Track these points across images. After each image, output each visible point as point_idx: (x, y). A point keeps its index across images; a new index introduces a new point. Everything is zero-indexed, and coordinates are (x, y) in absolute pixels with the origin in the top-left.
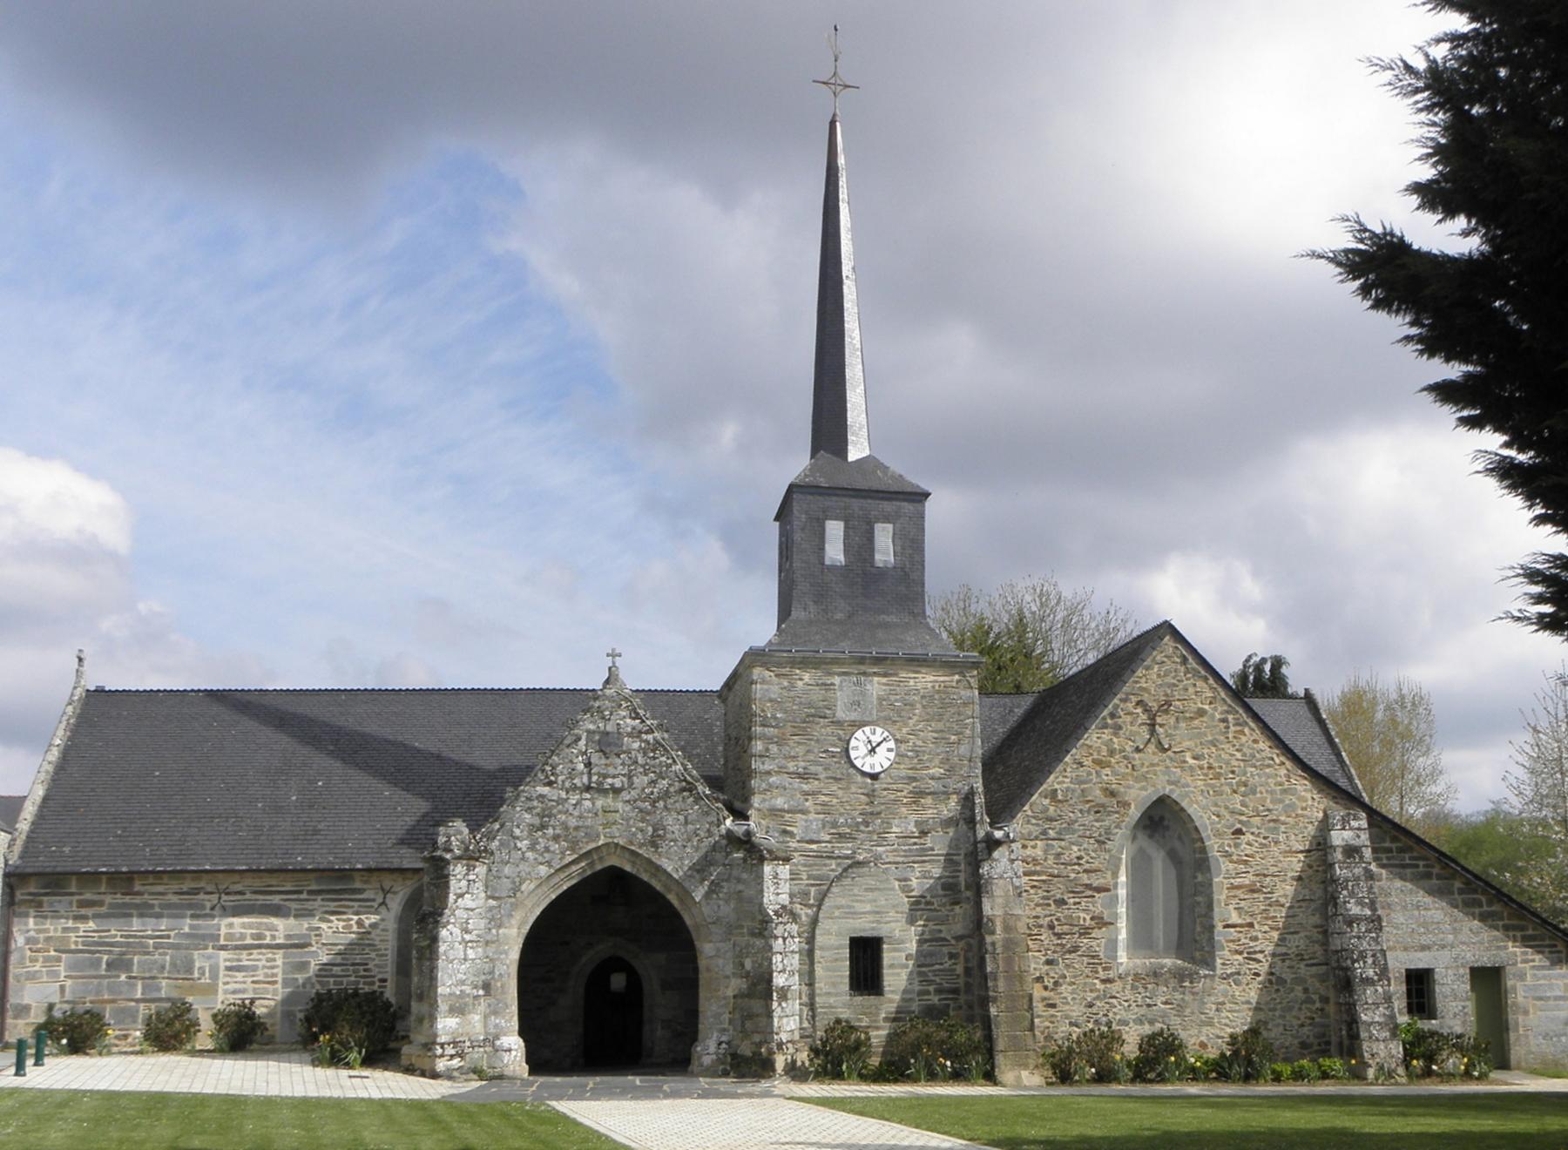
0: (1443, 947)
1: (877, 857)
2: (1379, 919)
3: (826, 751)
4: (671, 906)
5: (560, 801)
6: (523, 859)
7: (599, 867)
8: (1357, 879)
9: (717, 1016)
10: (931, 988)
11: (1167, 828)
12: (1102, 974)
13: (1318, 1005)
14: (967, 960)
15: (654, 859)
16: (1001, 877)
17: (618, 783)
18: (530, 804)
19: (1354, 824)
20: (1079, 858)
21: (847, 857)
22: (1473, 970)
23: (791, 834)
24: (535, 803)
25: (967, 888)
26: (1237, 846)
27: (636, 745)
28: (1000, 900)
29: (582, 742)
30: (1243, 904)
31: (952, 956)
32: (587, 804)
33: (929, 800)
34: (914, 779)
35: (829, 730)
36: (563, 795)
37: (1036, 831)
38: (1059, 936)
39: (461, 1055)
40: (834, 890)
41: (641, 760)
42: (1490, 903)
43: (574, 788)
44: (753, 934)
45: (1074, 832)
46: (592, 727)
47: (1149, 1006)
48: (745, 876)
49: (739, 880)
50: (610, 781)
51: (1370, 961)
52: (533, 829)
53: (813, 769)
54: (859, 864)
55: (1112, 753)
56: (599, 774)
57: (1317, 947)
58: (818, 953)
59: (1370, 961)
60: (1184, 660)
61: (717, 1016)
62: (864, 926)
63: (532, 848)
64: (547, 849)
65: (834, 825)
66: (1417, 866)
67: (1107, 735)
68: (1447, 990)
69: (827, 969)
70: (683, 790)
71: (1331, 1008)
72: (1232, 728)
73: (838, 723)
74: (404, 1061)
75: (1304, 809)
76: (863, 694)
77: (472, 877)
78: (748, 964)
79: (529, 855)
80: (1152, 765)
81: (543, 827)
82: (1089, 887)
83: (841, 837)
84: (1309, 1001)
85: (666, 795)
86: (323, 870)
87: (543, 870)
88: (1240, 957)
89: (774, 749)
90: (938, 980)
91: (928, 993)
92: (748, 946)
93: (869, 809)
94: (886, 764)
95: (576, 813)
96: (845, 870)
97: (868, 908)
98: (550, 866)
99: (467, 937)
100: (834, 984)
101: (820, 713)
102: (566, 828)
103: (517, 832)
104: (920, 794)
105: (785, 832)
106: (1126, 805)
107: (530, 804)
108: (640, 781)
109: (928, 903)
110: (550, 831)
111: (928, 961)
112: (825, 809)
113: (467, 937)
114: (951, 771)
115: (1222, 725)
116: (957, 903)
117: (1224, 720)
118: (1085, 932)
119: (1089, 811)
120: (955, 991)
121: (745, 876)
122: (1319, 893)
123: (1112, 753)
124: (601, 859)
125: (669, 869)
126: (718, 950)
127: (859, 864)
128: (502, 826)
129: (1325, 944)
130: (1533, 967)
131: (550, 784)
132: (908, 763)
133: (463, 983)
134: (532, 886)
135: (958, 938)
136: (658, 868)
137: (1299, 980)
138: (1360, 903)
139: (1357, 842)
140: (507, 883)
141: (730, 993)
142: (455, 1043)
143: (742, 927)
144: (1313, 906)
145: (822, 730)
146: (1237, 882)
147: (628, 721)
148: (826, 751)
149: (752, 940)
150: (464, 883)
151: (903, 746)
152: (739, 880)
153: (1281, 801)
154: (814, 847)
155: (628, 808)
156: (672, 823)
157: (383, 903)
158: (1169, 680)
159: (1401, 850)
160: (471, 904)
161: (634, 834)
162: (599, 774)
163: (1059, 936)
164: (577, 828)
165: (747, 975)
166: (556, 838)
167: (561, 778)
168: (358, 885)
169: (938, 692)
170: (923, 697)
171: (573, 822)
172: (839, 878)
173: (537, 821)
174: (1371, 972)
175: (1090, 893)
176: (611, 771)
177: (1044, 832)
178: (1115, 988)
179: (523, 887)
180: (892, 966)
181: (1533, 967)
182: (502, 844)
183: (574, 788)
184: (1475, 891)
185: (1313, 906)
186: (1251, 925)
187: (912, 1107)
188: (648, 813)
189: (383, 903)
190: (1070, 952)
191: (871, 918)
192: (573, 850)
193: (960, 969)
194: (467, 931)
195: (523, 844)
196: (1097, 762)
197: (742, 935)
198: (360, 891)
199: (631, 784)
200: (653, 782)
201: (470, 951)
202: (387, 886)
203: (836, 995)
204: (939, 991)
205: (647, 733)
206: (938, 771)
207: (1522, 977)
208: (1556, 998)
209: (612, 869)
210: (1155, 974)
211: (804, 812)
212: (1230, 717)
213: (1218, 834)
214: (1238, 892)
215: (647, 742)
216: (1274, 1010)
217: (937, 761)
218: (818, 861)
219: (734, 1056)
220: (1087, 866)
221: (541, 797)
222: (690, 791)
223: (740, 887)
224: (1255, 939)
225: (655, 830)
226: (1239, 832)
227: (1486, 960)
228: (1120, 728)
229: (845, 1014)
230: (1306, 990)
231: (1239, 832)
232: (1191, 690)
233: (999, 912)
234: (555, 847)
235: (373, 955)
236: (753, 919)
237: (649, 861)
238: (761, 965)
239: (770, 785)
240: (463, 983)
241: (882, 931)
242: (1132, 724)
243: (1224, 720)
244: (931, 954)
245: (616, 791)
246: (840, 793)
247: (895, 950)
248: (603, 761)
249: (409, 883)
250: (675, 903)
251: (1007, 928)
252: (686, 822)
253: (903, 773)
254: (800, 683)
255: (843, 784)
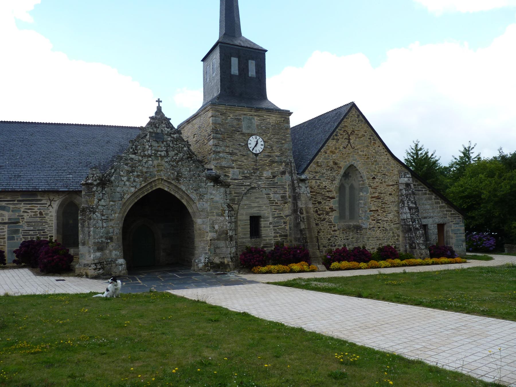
0: (430, 217)
1: (259, 185)
2: (418, 208)
3: (240, 145)
4: (184, 204)
5: (140, 161)
6: (125, 185)
7: (154, 189)
8: (410, 194)
9: (204, 248)
10: (278, 235)
11: (350, 176)
12: (333, 229)
13: (397, 238)
14: (290, 225)
15: (178, 185)
16: (303, 193)
17: (163, 154)
18: (127, 162)
19: (408, 176)
20: (326, 187)
21: (248, 186)
22: (438, 224)
23: (228, 176)
24: (129, 161)
25: (289, 197)
26: (373, 183)
27: (169, 139)
28: (304, 202)
29: (148, 137)
30: (375, 203)
31: (285, 223)
32: (150, 162)
33: (275, 165)
34: (270, 156)
35: (240, 136)
36: (140, 158)
37: (312, 176)
38: (319, 215)
39: (103, 268)
40: (244, 198)
41: (171, 145)
42: (442, 203)
43: (145, 156)
44: (218, 215)
45: (324, 177)
46: (152, 131)
47: (347, 239)
48: (214, 192)
49: (211, 194)
50: (159, 153)
51: (417, 222)
52: (128, 172)
53: (235, 151)
54: (253, 188)
55: (336, 149)
56: (155, 150)
57: (396, 218)
58: (239, 222)
59: (417, 222)
60: (358, 116)
61: (204, 248)
62: (254, 211)
63: (128, 180)
64: (134, 181)
65: (243, 173)
66: (422, 191)
67: (334, 142)
68: (431, 232)
69: (242, 228)
70: (188, 158)
71: (401, 239)
72: (372, 142)
73: (243, 134)
74: (77, 272)
75: (393, 170)
76: (251, 123)
77: (104, 192)
78: (217, 227)
79: (127, 183)
80: (348, 154)
81: (133, 172)
82: (328, 197)
83: (246, 177)
84: (394, 236)
85: (182, 159)
86: (25, 191)
87: (133, 190)
88: (374, 222)
89: (221, 143)
90: (280, 231)
91: (277, 237)
92: (216, 219)
93: (255, 167)
94: (261, 150)
95: (146, 166)
96: (248, 190)
97: (256, 205)
98: (136, 188)
99: (103, 218)
100: (245, 234)
101: (237, 130)
102: (142, 172)
103: (122, 173)
104: (273, 162)
105: (226, 175)
106: (340, 168)
107: (127, 162)
108: (171, 153)
109: (276, 203)
110: (135, 173)
111: (277, 225)
112: (240, 167)
113: (103, 218)
114: (282, 154)
115: (369, 140)
116: (286, 203)
117: (370, 139)
118: (327, 213)
119: (328, 170)
120: (286, 236)
121: (214, 192)
122: (397, 199)
123: (336, 149)
124: (156, 185)
125: (184, 189)
126: (203, 222)
127: (253, 188)
128: (115, 170)
129: (398, 217)
130: (454, 224)
131: (135, 154)
132: (268, 150)
133: (102, 237)
134: (129, 196)
135: (287, 216)
136: (179, 189)
137: (391, 229)
138: (412, 203)
139: (409, 182)
140: (118, 195)
141: (209, 239)
142: (100, 263)
143: (214, 212)
144: (395, 204)
145: (237, 136)
146: (373, 195)
147: (166, 129)
148: (240, 145)
149: (218, 218)
150: (101, 195)
151: (266, 144)
152: (211, 194)
153: (386, 168)
154: (236, 181)
155: (167, 164)
156: (185, 171)
157: (50, 205)
158: (354, 123)
159: (418, 185)
160: (104, 204)
161: (170, 175)
162: (155, 150)
163: (319, 215)
164: (146, 172)
165: (216, 232)
166: (138, 176)
167: (139, 151)
168: (39, 198)
169: (277, 124)
170: (272, 126)
171: (145, 170)
172: (245, 194)
173: (130, 169)
174: (418, 226)
175: (329, 199)
176: (160, 149)
177: (314, 177)
178: (337, 233)
179: (125, 197)
180: (264, 227)
181: (454, 224)
182: (115, 178)
183: (145, 156)
184: (438, 199)
185: (395, 204)
186: (377, 210)
187: (447, 306)
188: (176, 167)
189: (50, 205)
190: (323, 221)
191: (257, 209)
192: (145, 182)
193: (287, 228)
194: (103, 215)
195: (125, 179)
196: (332, 152)
197: (214, 216)
198: (41, 200)
199: (168, 155)
200: (177, 154)
201: (104, 224)
202: (51, 198)
203: (246, 238)
204: (280, 236)
205: (173, 134)
206: (278, 154)
207: (451, 227)
208: (460, 233)
209: (160, 189)
210: (349, 229)
211: (233, 168)
212: (372, 138)
213: (368, 179)
214: (374, 199)
215: (173, 137)
216: (384, 240)
217: (278, 150)
218: (238, 187)
219: (212, 263)
220: (328, 190)
221: (132, 159)
222: (191, 158)
223: (212, 197)
224: (378, 215)
225: (178, 174)
226: (374, 178)
227: (441, 221)
228: (339, 140)
229: (249, 245)
230: (393, 233)
231: (374, 178)
232: (360, 127)
233: (303, 206)
234: (137, 180)
235: (47, 226)
236: (219, 209)
237: (176, 186)
238: (222, 227)
239: (220, 157)
240: (102, 237)
241: (262, 213)
242: (342, 138)
243: (370, 139)
244: (278, 222)
245: (162, 157)
246: (245, 161)
247: (266, 221)
248: (157, 145)
249: (61, 197)
250: (185, 203)
251: (307, 212)
252: (190, 171)
253: (267, 154)
254: (229, 118)
255: (246, 157)
